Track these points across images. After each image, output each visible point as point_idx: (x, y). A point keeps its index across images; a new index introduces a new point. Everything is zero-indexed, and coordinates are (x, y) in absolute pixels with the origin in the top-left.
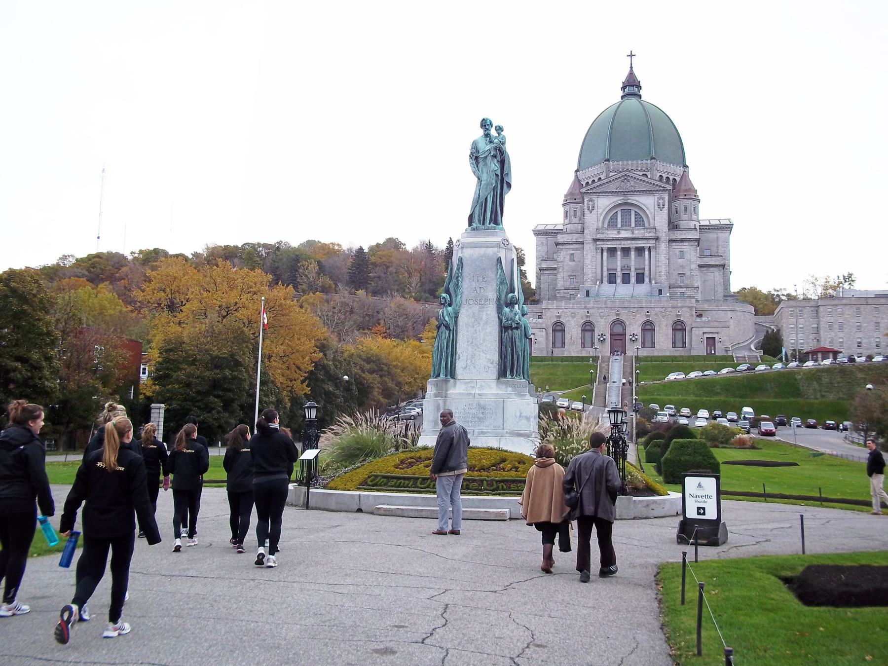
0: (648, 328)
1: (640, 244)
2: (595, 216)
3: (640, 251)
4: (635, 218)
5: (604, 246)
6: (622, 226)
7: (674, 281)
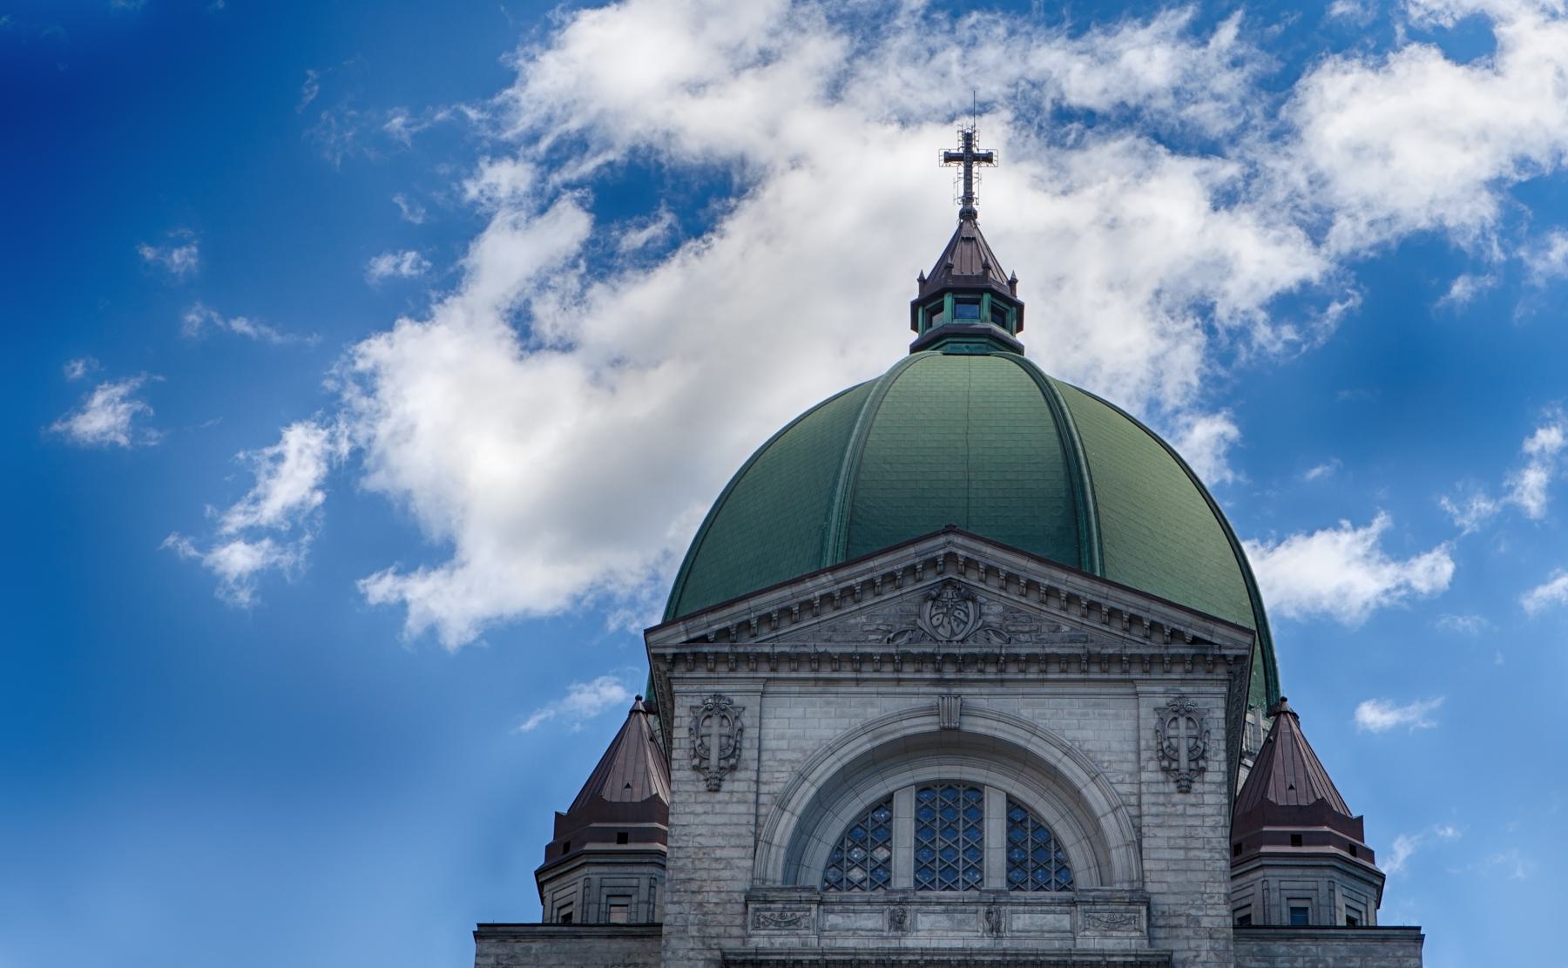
4: (1012, 845)
6: (919, 885)
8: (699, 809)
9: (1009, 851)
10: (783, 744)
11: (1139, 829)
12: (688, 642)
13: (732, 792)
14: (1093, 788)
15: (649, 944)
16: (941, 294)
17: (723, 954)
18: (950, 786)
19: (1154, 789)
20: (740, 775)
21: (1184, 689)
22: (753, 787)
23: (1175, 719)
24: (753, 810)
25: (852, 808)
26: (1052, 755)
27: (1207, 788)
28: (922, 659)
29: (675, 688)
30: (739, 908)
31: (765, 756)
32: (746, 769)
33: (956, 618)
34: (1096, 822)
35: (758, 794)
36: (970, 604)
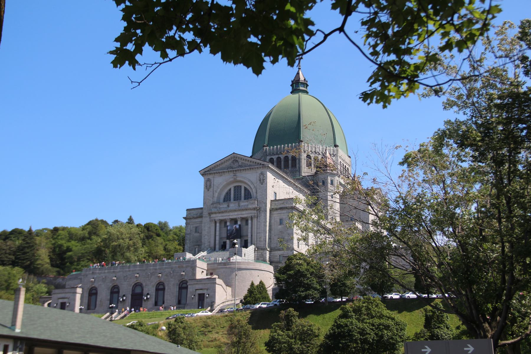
0: (160, 288)
1: (245, 214)
2: (211, 193)
3: (246, 220)
5: (217, 219)
7: (275, 245)
11: (256, 190)
18: (238, 186)
25: (226, 190)
28: (231, 171)
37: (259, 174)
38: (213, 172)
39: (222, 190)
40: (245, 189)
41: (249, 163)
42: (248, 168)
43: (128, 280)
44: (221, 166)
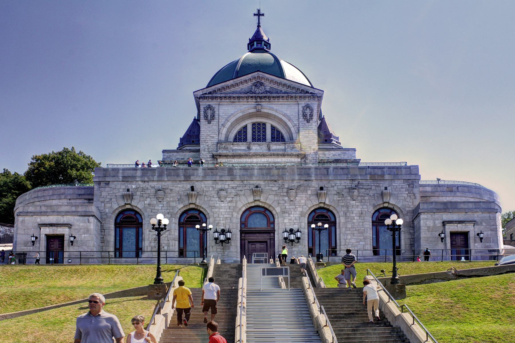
2: (216, 128)
8: (206, 127)
9: (271, 135)
10: (224, 115)
12: (203, 94)
13: (213, 124)
14: (289, 122)
15: (198, 153)
16: (254, 42)
17: (213, 154)
18: (259, 124)
19: (302, 122)
20: (214, 121)
21: (308, 103)
22: (218, 123)
23: (307, 109)
24: (218, 127)
26: (281, 116)
27: (313, 122)
28: (252, 97)
29: (200, 104)
30: (216, 146)
31: (220, 117)
32: (216, 119)
33: (260, 89)
34: (290, 129)
35: (219, 124)
36: (263, 86)
37: (303, 107)
38: (219, 95)
39: (233, 126)
40: (273, 128)
41: (284, 89)
42: (286, 95)
43: (228, 199)
44: (232, 89)
